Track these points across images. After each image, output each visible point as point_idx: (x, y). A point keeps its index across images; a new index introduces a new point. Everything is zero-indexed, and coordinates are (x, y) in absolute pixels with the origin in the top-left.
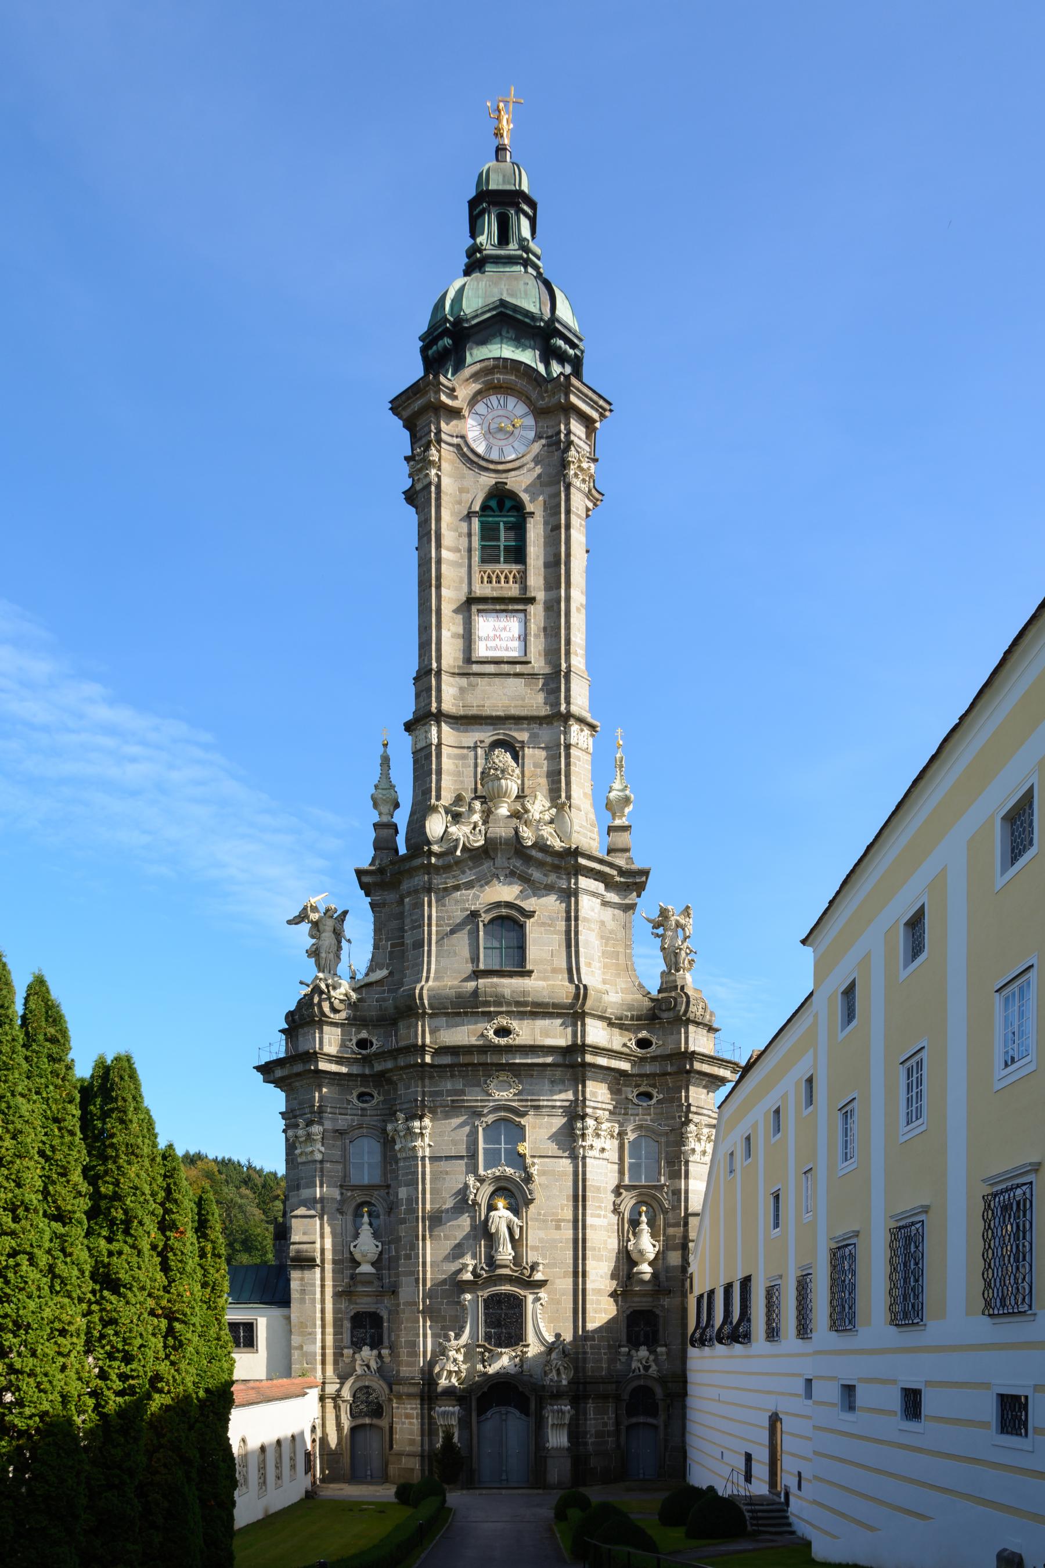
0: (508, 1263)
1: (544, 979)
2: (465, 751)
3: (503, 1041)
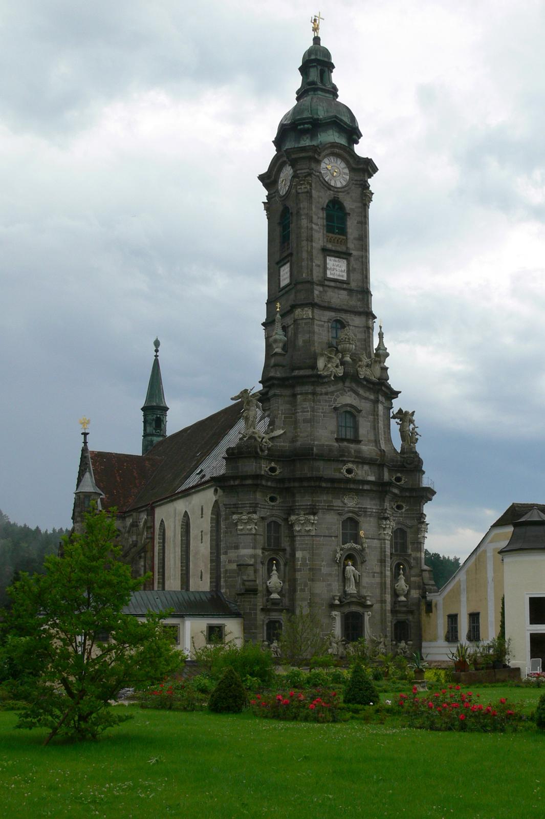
0: (355, 595)
1: (366, 445)
2: (323, 323)
3: (350, 476)
